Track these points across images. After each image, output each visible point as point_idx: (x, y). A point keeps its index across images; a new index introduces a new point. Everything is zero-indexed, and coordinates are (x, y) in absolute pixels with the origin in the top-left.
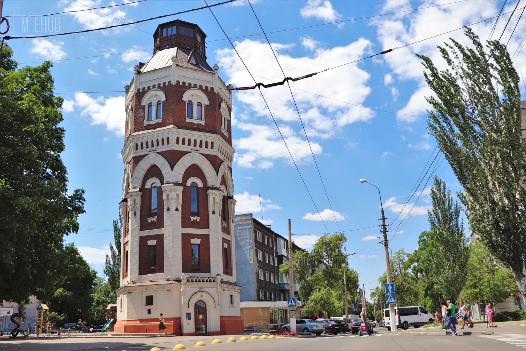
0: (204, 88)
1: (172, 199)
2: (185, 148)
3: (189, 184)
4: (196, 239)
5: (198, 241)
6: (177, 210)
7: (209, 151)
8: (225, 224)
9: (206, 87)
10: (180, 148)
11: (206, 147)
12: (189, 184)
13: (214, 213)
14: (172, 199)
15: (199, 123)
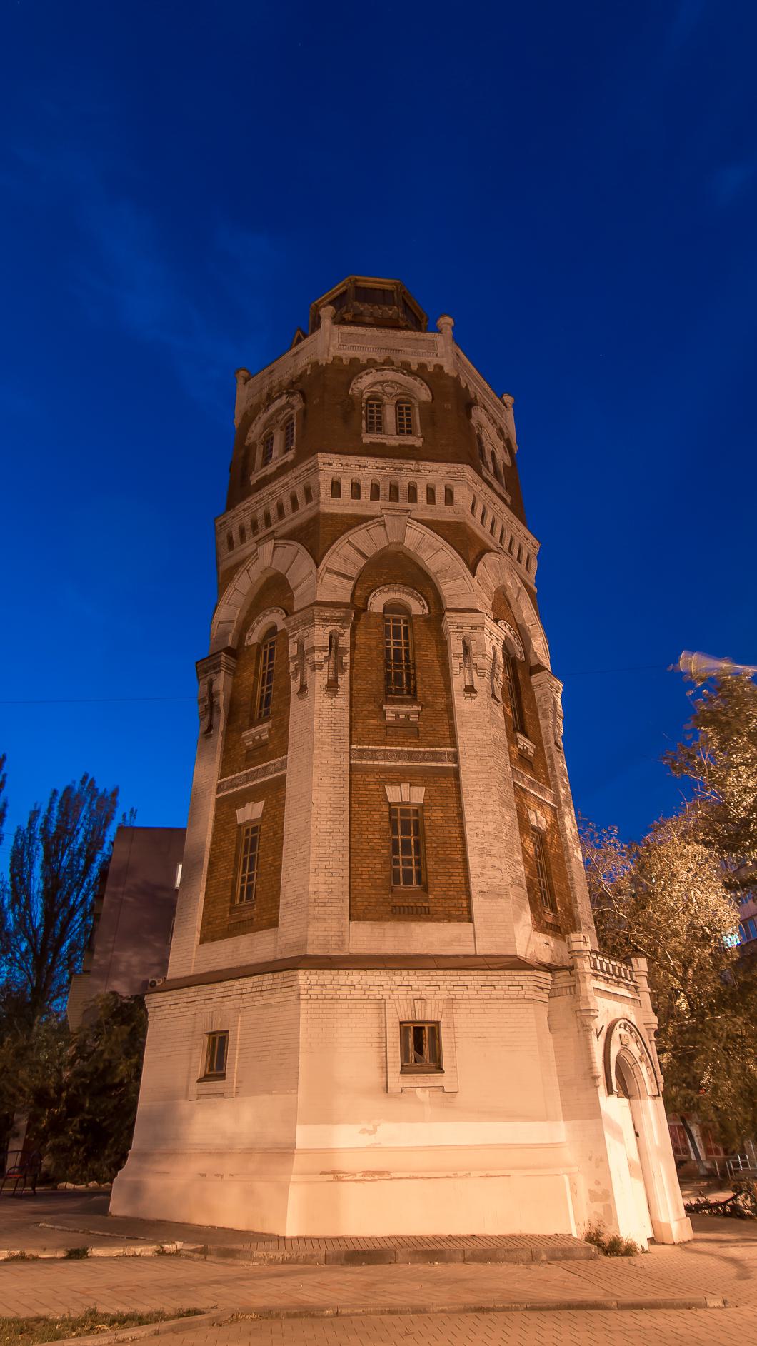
0: (414, 367)
1: (313, 649)
2: (364, 505)
3: (377, 603)
4: (405, 787)
5: (417, 795)
6: (332, 686)
7: (441, 512)
8: (525, 743)
9: (422, 366)
10: (344, 506)
11: (431, 498)
12: (377, 603)
13: (470, 689)
14: (313, 649)
15: (402, 443)
